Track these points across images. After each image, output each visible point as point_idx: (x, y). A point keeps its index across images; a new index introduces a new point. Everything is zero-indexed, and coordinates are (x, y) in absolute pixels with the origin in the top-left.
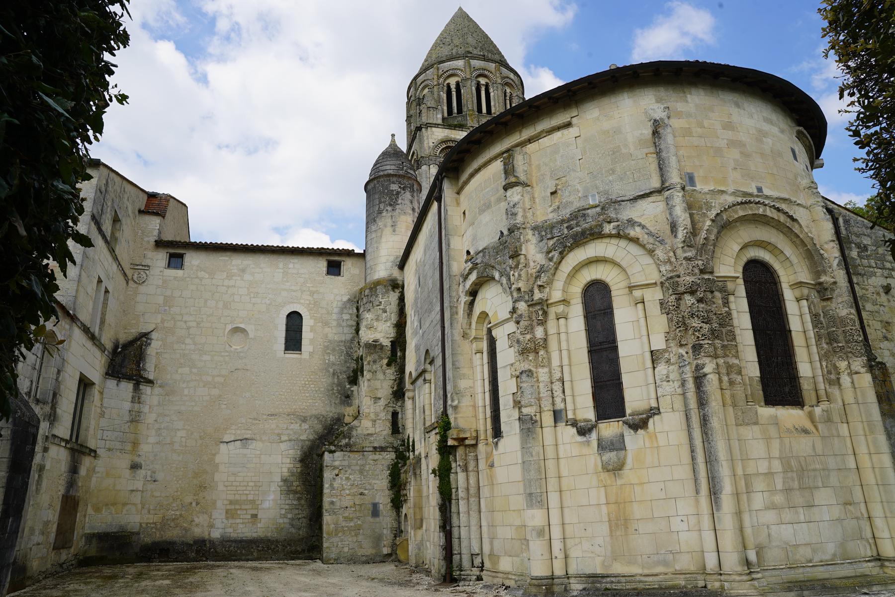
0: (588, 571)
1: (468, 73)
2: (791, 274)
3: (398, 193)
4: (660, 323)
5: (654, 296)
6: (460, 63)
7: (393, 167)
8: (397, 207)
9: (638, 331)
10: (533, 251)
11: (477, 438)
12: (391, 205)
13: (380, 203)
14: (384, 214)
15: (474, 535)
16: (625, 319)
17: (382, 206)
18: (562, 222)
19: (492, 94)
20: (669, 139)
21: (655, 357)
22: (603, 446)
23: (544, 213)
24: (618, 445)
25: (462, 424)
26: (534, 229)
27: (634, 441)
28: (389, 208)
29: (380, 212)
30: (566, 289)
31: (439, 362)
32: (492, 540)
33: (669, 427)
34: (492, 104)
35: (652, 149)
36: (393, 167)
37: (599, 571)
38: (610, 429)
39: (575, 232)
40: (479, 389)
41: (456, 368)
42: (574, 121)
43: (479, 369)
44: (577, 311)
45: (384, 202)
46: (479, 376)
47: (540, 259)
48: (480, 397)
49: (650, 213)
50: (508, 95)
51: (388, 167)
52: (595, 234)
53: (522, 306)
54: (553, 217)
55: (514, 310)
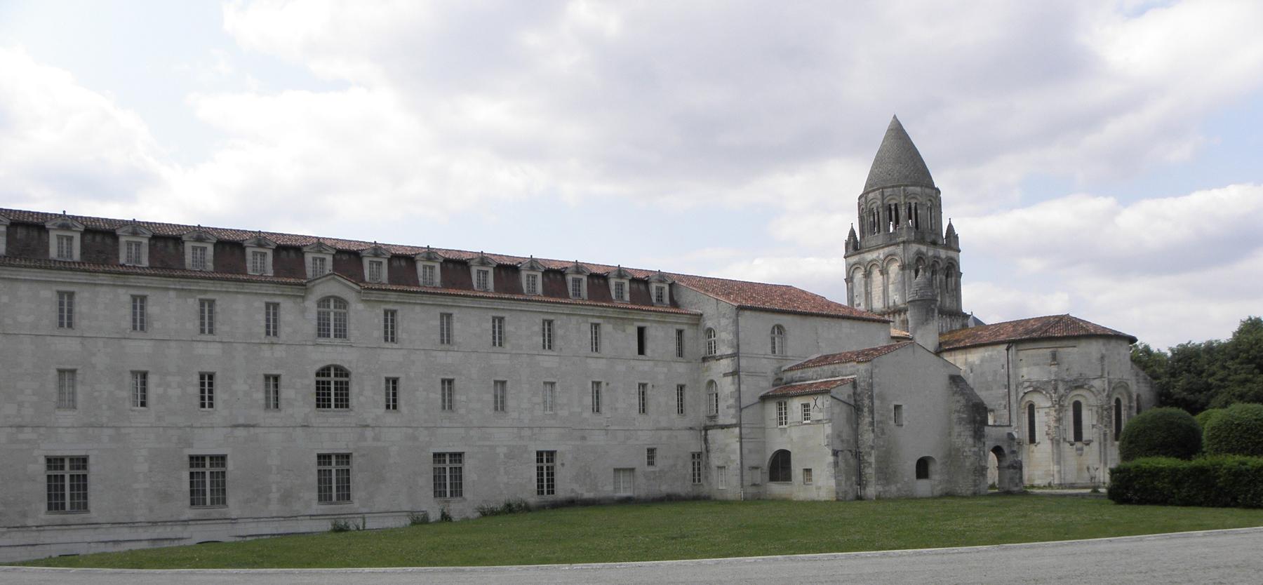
2: (1124, 402)
4: (1096, 417)
5: (1095, 409)
6: (918, 189)
9: (1088, 418)
10: (1061, 389)
16: (1086, 415)
20: (1106, 362)
21: (1093, 426)
22: (1077, 449)
24: (1081, 449)
27: (1086, 448)
30: (1068, 403)
33: (1095, 445)
38: (1079, 444)
39: (1078, 384)
44: (1071, 408)
49: (1097, 384)
52: (1081, 387)
54: (1067, 378)
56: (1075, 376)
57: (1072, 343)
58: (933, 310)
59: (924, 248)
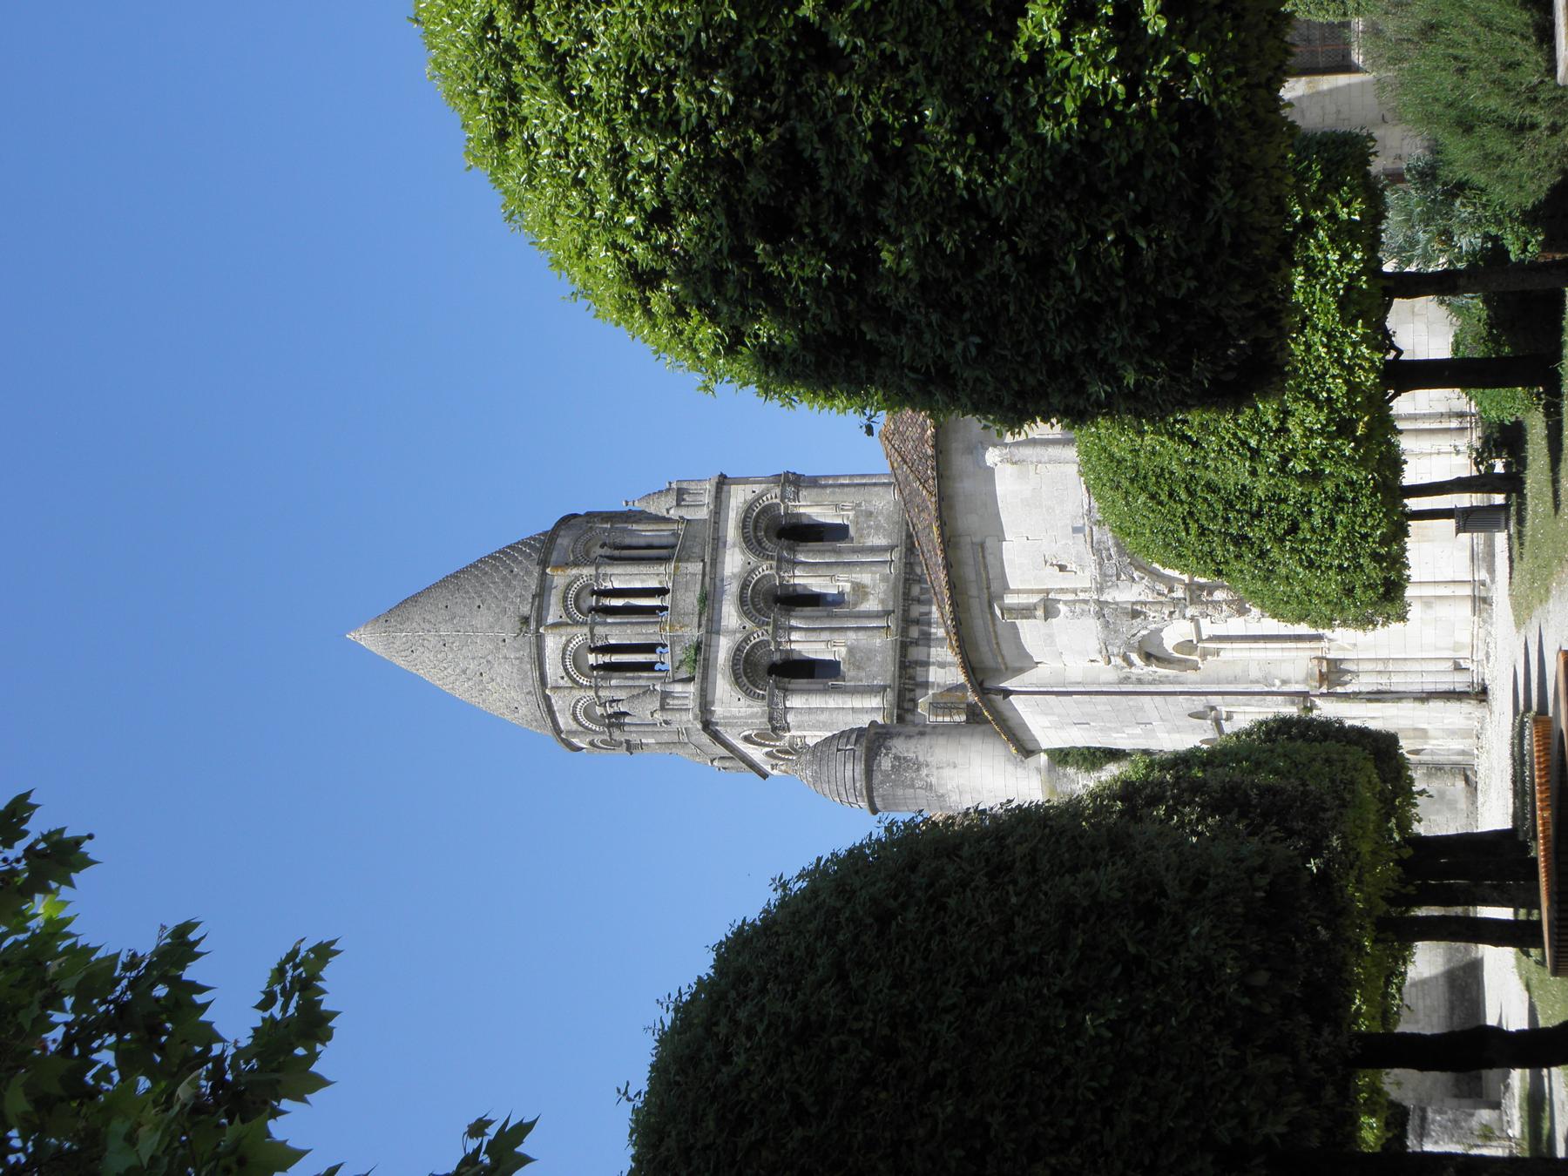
0: (1467, 561)
1: (575, 630)
3: (897, 758)
6: (553, 644)
7: (849, 766)
8: (921, 759)
11: (1320, 659)
12: (918, 769)
13: (912, 786)
14: (934, 780)
15: (1432, 667)
17: (918, 783)
18: (1101, 565)
19: (617, 585)
23: (1084, 577)
25: (1301, 675)
26: (1100, 590)
28: (924, 772)
29: (929, 787)
31: (1215, 700)
32: (1437, 649)
34: (638, 585)
35: (1032, 468)
36: (849, 766)
37: (1468, 553)
40: (1262, 655)
41: (1236, 680)
42: (977, 539)
43: (1236, 654)
45: (912, 780)
46: (1246, 654)
47: (1136, 588)
48: (1271, 655)
50: (607, 551)
51: (849, 774)
53: (1190, 611)
54: (1092, 570)
55: (1192, 619)
56: (1080, 546)
57: (966, 553)
58: (901, 762)
59: (724, 647)
